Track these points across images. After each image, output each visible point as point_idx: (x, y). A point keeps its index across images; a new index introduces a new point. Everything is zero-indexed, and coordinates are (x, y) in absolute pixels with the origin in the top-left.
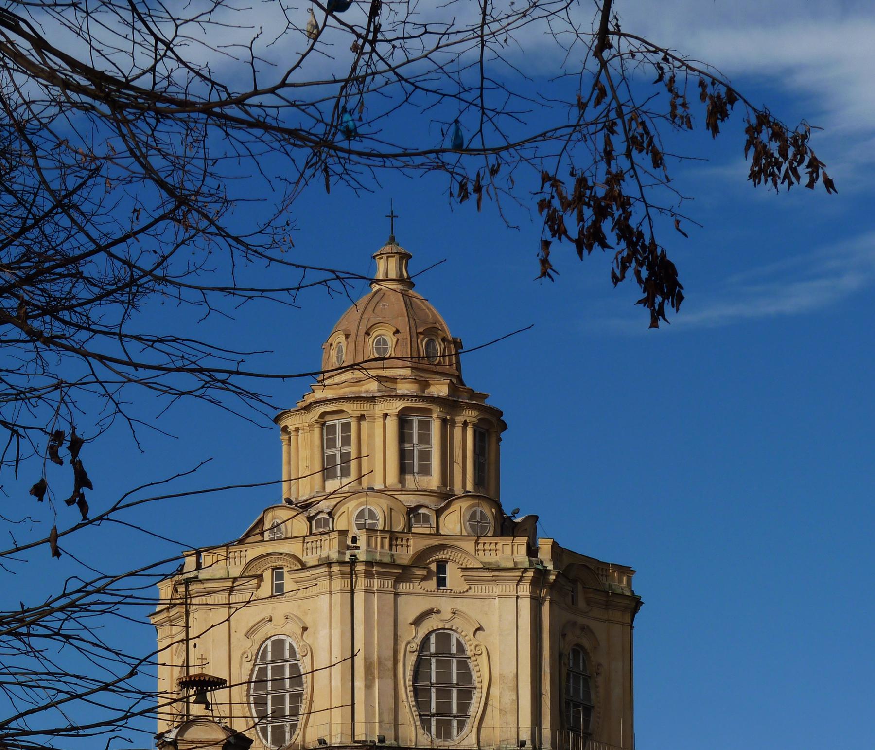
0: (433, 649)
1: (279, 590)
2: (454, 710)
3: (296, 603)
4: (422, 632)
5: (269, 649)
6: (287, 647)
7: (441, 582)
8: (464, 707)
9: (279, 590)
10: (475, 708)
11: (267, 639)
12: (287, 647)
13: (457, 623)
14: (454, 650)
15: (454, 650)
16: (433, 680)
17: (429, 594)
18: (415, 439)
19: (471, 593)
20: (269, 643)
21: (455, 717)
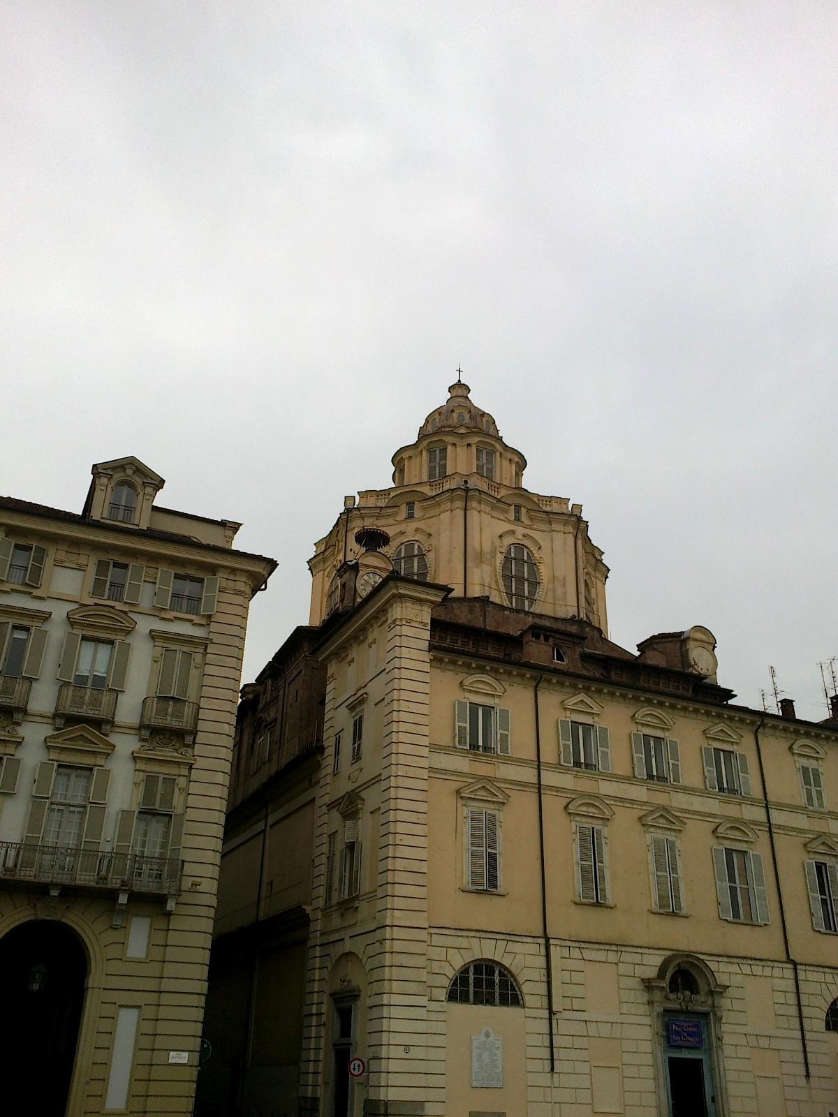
0: (513, 555)
1: (411, 516)
2: (526, 594)
3: (423, 521)
4: (508, 540)
5: (403, 550)
6: (416, 547)
7: (518, 519)
8: (532, 592)
9: (411, 516)
10: (540, 593)
11: (402, 544)
12: (416, 547)
13: (526, 542)
14: (525, 558)
15: (525, 558)
16: (513, 573)
17: (510, 522)
18: (485, 461)
19: (535, 527)
20: (403, 547)
21: (527, 598)
